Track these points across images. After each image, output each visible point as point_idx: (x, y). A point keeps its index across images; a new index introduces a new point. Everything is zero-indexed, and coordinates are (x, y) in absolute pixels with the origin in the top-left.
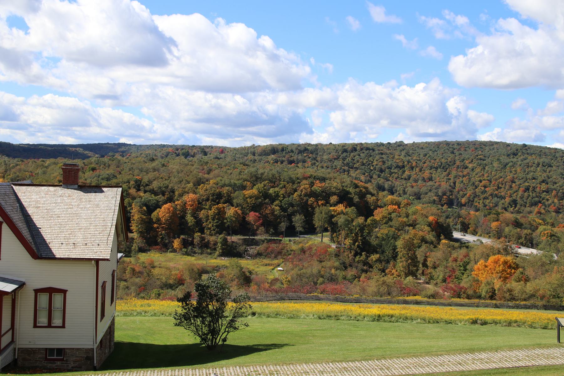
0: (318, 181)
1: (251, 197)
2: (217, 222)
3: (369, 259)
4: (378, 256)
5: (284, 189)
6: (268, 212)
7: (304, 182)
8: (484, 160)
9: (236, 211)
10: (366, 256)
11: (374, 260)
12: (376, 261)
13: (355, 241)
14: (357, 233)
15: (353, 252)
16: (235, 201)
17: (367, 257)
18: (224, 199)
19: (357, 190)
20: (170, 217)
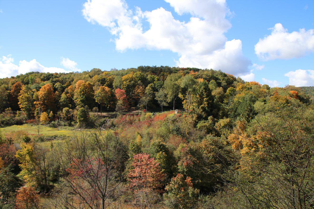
0: (192, 71)
1: (126, 80)
2: (82, 97)
3: (217, 124)
4: (228, 120)
5: (162, 76)
6: (140, 91)
7: (181, 71)
8: (306, 92)
9: (104, 90)
10: (213, 120)
11: (222, 125)
12: (225, 127)
13: (200, 103)
14: (202, 93)
15: (195, 116)
16: (114, 84)
17: (214, 122)
18: (107, 83)
19: (226, 78)
20: (45, 94)
